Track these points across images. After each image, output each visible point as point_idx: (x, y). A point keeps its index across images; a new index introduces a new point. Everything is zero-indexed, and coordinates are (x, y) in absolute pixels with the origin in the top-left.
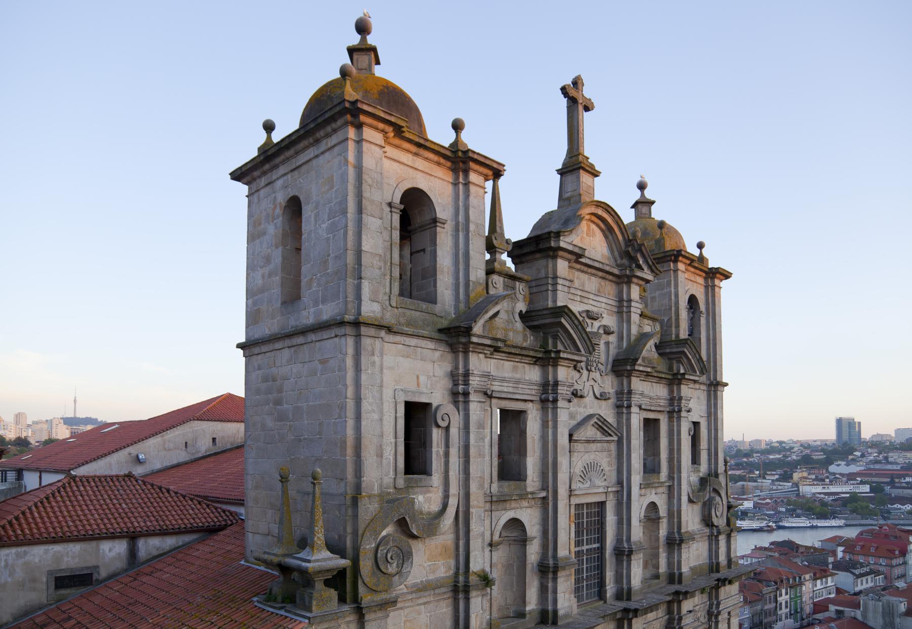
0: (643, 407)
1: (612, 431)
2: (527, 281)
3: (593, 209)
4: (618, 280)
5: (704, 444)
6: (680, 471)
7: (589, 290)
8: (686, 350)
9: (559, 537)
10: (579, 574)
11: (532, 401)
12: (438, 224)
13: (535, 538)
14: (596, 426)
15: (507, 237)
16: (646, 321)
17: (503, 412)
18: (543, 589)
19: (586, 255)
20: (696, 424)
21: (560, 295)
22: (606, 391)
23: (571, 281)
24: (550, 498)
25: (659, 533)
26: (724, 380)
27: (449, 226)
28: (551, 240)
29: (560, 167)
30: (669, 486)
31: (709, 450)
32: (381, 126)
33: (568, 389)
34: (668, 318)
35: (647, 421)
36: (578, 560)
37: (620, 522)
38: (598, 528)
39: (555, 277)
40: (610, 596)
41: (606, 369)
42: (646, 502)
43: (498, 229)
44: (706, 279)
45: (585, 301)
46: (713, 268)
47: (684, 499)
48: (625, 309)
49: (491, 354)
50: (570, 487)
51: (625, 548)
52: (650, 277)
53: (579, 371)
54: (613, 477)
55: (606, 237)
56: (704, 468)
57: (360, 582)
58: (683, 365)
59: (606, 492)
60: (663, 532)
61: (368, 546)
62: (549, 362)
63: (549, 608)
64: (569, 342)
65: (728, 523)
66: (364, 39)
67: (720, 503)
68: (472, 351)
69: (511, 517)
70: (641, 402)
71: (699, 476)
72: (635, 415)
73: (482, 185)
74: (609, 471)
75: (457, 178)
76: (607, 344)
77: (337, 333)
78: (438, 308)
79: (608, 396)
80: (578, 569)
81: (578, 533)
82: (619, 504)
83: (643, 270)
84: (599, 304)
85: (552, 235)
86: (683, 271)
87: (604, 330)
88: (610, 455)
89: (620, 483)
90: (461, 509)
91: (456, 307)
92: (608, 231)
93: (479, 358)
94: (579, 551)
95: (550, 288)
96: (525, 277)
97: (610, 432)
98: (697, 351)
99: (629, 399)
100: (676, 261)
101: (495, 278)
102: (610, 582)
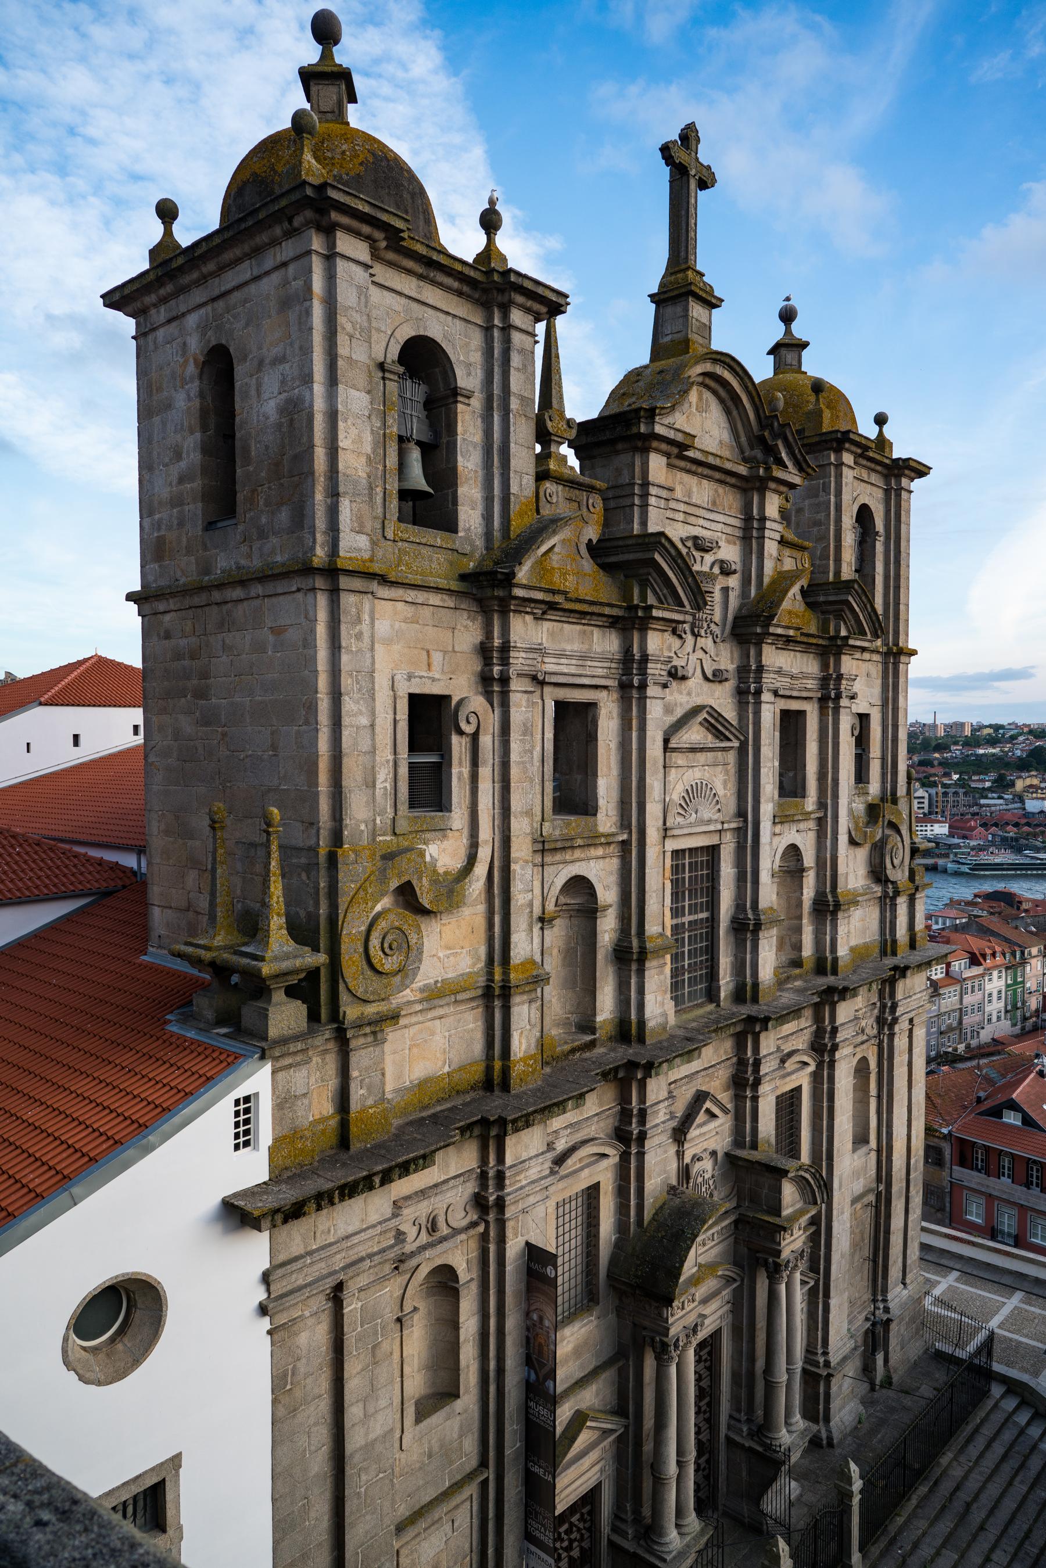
0: (781, 693)
1: (731, 732)
2: (599, 491)
3: (708, 367)
4: (744, 485)
5: (875, 750)
6: (836, 796)
7: (699, 502)
8: (850, 599)
9: (647, 903)
10: (677, 962)
11: (605, 687)
12: (460, 399)
13: (611, 906)
14: (706, 725)
15: (569, 415)
16: (787, 552)
17: (561, 707)
18: (622, 988)
19: (696, 445)
20: (863, 719)
21: (652, 512)
22: (722, 668)
23: (671, 490)
24: (634, 844)
25: (802, 894)
26: (911, 645)
27: (477, 403)
28: (639, 422)
29: (655, 290)
30: (819, 819)
31: (883, 759)
32: (366, 229)
33: (663, 667)
35: (785, 714)
36: (677, 940)
38: (707, 888)
39: (646, 484)
40: (726, 996)
41: (723, 633)
42: (782, 843)
43: (554, 402)
44: (886, 477)
45: (692, 520)
46: (899, 459)
47: (843, 839)
48: (755, 533)
49: (544, 613)
50: (665, 823)
52: (797, 480)
53: (680, 637)
54: (730, 805)
55: (728, 412)
56: (874, 787)
57: (342, 987)
58: (845, 623)
59: (720, 831)
60: (808, 892)
61: (353, 928)
62: (634, 624)
64: (665, 591)
65: (912, 878)
66: (326, 55)
67: (900, 845)
68: (515, 611)
69: (573, 874)
70: (778, 685)
71: (866, 802)
72: (768, 706)
73: (530, 329)
74: (725, 795)
75: (490, 318)
76: (726, 590)
77: (299, 586)
79: (725, 675)
80: (677, 954)
81: (676, 896)
83: (786, 467)
84: (713, 526)
85: (642, 413)
86: (850, 467)
87: (721, 568)
88: (727, 772)
89: (741, 813)
90: (496, 863)
92: (730, 402)
93: (525, 622)
94: (677, 925)
95: (637, 501)
96: (598, 484)
97: (727, 733)
98: (869, 600)
99: (759, 680)
100: (838, 451)
101: (549, 486)
102: (725, 974)
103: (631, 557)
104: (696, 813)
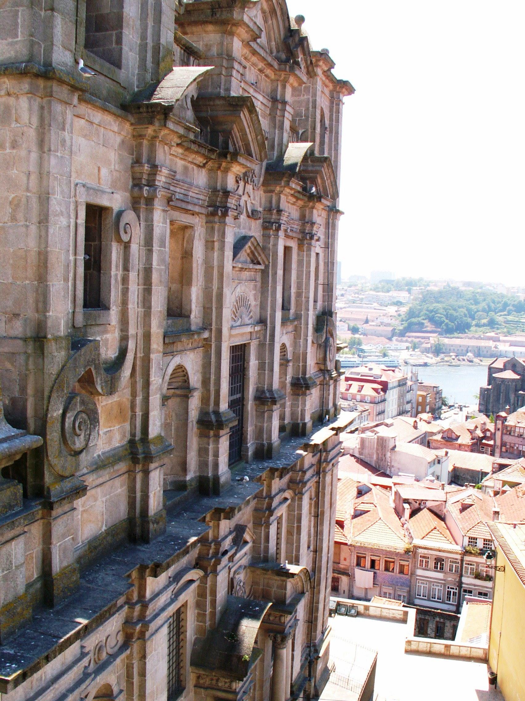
6: (308, 310)
21: (234, 83)
34: (304, 130)
37: (261, 367)
48: (279, 113)
63: (210, 475)
78: (122, 75)
82: (261, 345)
104: (241, 318)
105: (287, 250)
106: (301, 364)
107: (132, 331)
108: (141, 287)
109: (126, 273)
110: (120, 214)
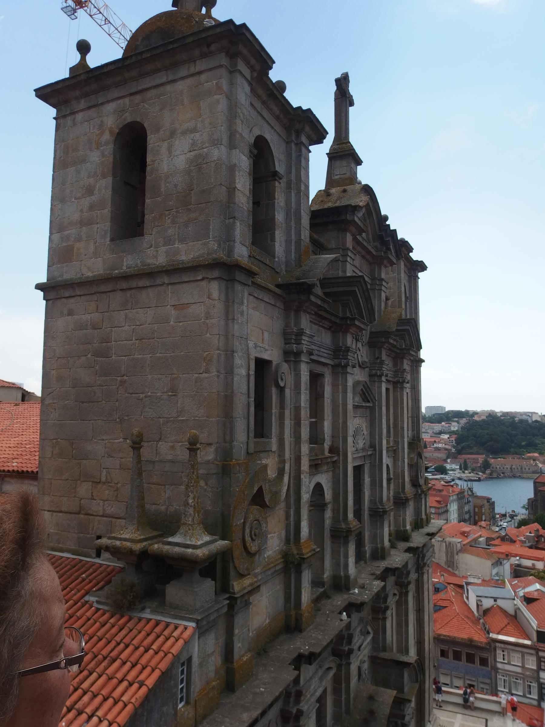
1: (370, 398)
37: (373, 484)
51: (380, 509)
91: (287, 263)
103: (340, 289)
105: (387, 389)
106: (400, 481)
107: (287, 455)
108: (293, 422)
109: (282, 411)
110: (278, 366)
